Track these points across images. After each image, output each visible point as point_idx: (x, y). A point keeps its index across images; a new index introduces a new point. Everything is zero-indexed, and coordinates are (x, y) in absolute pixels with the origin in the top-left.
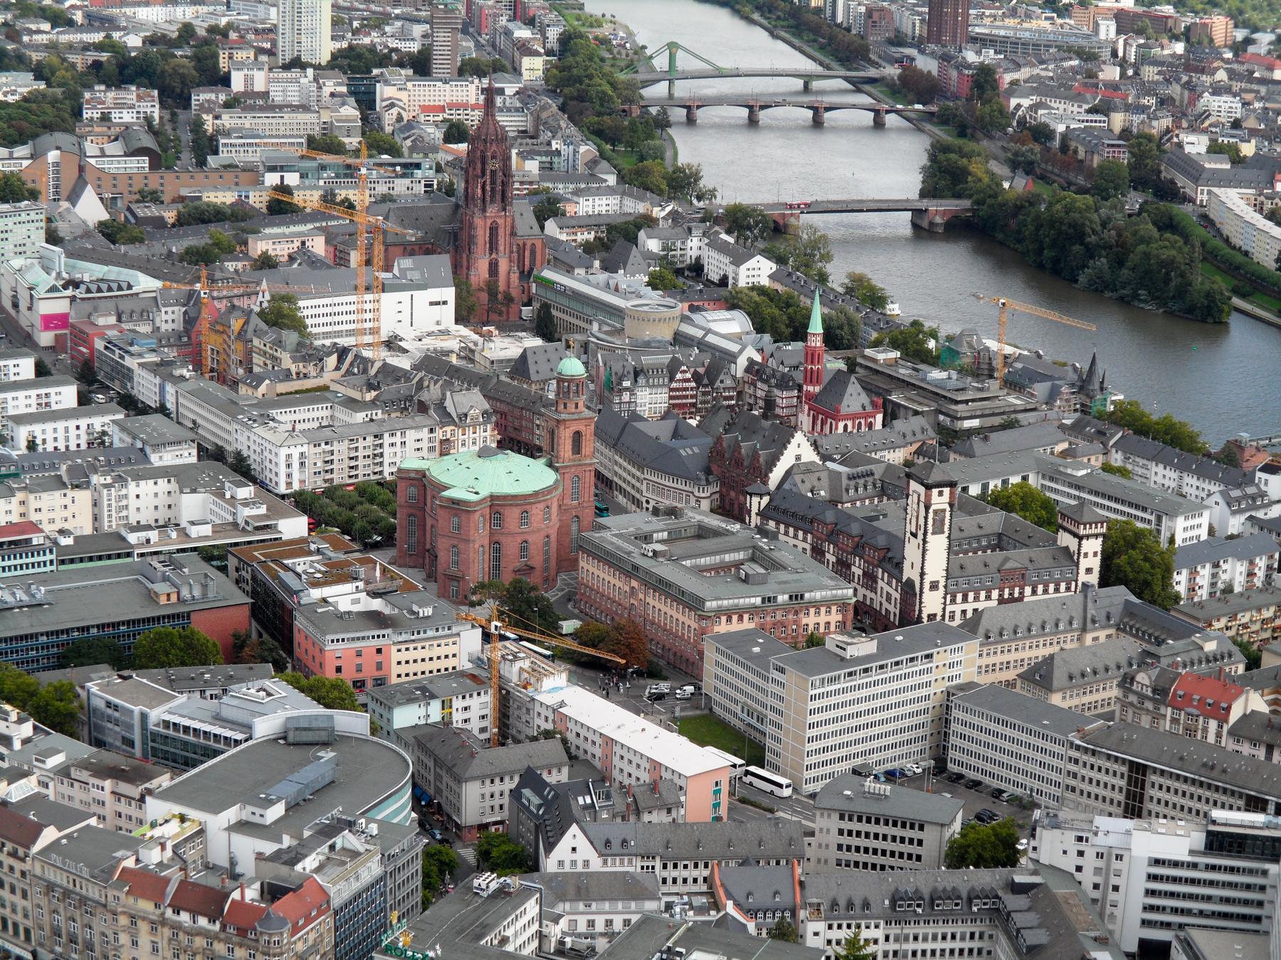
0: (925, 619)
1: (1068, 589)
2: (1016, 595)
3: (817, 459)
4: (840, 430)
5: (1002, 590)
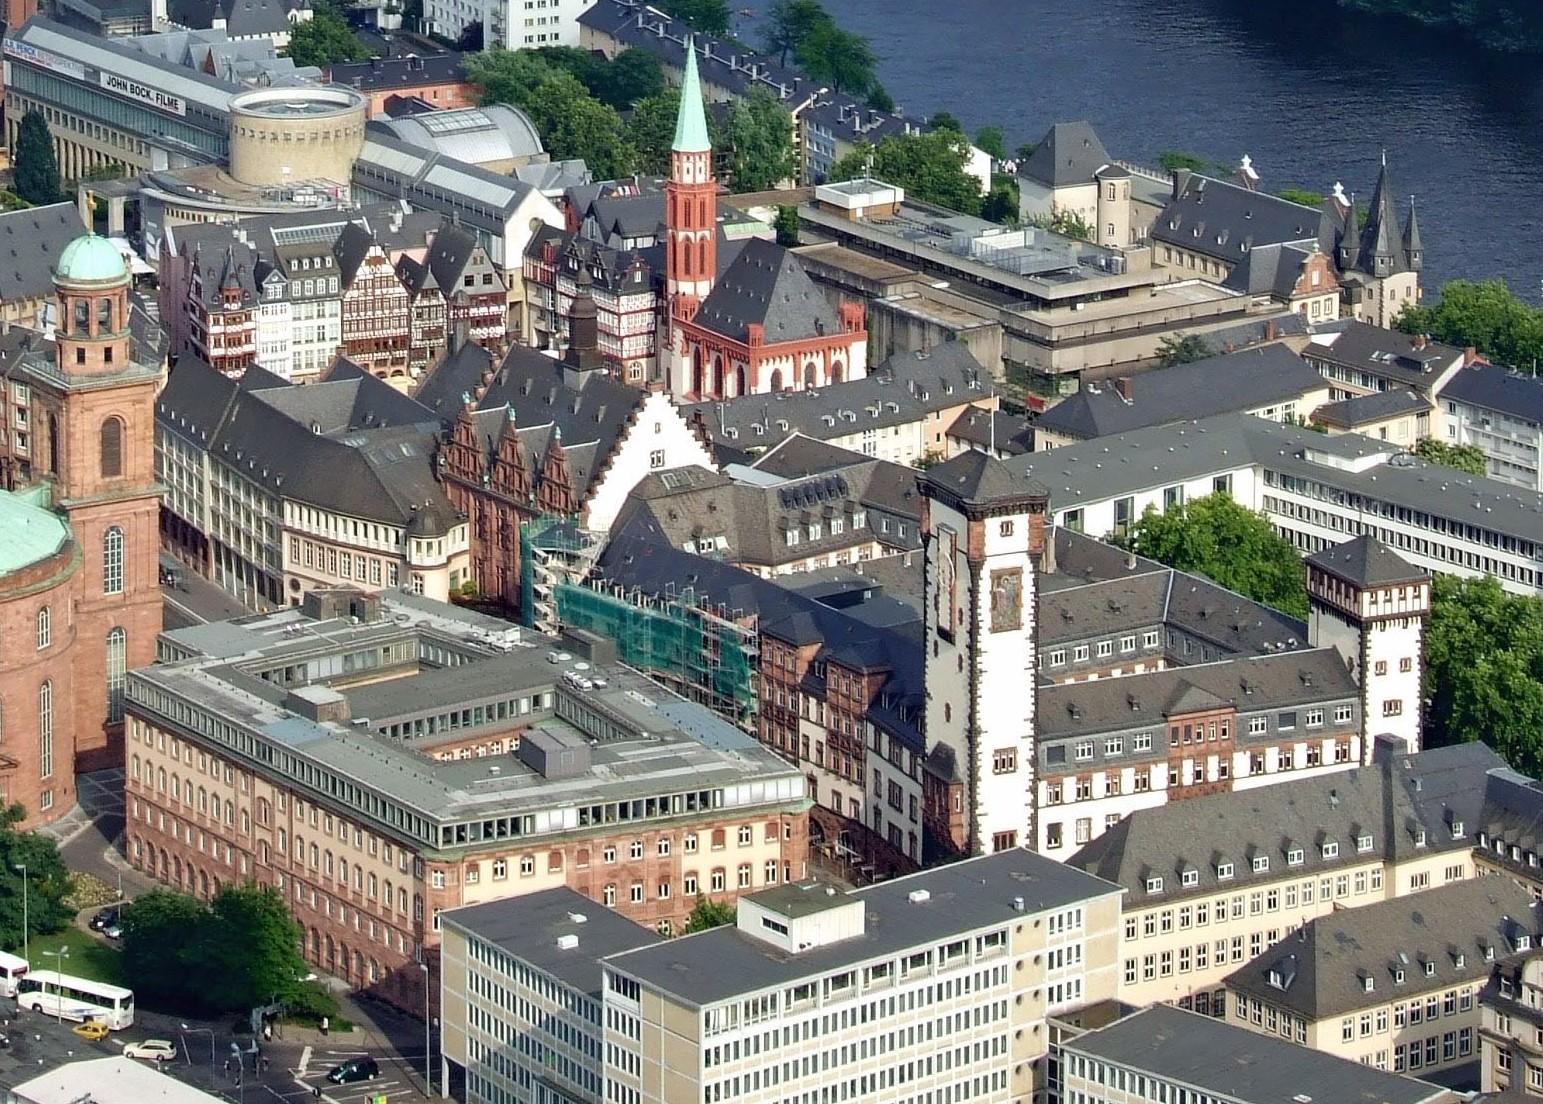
0: (988, 848)
1: (1342, 755)
2: (1213, 776)
3: (704, 460)
4: (764, 386)
5: (1175, 764)
